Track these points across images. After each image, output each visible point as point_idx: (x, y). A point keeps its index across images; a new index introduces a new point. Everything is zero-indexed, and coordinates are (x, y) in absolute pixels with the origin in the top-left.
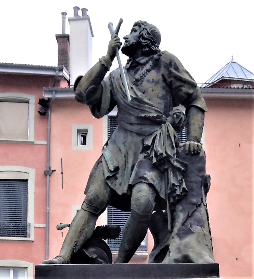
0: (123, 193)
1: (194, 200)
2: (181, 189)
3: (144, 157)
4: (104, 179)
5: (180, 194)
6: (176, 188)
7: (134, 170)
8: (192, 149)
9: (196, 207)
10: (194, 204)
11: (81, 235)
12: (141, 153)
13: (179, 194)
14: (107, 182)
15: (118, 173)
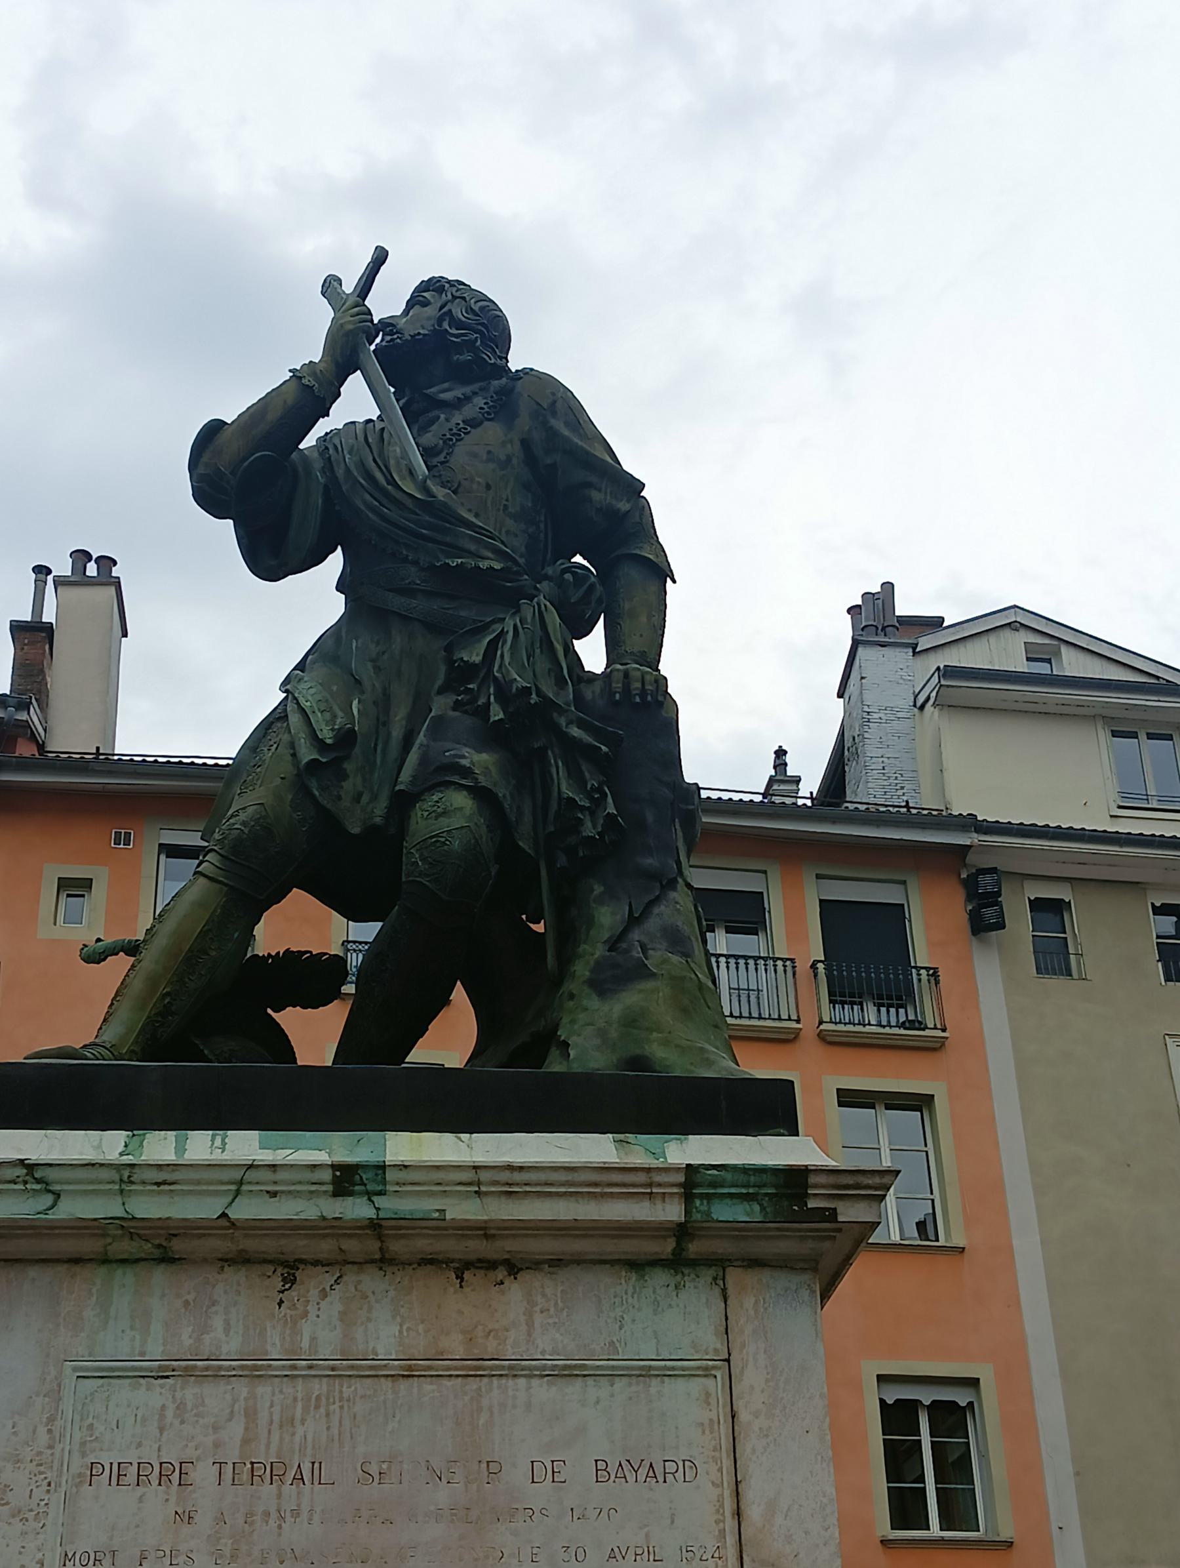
1: (650, 862)
2: (602, 821)
3: (452, 704)
4: (295, 772)
6: (580, 815)
7: (414, 749)
8: (637, 688)
10: (654, 876)
12: (439, 693)
13: (593, 837)
15: (347, 757)
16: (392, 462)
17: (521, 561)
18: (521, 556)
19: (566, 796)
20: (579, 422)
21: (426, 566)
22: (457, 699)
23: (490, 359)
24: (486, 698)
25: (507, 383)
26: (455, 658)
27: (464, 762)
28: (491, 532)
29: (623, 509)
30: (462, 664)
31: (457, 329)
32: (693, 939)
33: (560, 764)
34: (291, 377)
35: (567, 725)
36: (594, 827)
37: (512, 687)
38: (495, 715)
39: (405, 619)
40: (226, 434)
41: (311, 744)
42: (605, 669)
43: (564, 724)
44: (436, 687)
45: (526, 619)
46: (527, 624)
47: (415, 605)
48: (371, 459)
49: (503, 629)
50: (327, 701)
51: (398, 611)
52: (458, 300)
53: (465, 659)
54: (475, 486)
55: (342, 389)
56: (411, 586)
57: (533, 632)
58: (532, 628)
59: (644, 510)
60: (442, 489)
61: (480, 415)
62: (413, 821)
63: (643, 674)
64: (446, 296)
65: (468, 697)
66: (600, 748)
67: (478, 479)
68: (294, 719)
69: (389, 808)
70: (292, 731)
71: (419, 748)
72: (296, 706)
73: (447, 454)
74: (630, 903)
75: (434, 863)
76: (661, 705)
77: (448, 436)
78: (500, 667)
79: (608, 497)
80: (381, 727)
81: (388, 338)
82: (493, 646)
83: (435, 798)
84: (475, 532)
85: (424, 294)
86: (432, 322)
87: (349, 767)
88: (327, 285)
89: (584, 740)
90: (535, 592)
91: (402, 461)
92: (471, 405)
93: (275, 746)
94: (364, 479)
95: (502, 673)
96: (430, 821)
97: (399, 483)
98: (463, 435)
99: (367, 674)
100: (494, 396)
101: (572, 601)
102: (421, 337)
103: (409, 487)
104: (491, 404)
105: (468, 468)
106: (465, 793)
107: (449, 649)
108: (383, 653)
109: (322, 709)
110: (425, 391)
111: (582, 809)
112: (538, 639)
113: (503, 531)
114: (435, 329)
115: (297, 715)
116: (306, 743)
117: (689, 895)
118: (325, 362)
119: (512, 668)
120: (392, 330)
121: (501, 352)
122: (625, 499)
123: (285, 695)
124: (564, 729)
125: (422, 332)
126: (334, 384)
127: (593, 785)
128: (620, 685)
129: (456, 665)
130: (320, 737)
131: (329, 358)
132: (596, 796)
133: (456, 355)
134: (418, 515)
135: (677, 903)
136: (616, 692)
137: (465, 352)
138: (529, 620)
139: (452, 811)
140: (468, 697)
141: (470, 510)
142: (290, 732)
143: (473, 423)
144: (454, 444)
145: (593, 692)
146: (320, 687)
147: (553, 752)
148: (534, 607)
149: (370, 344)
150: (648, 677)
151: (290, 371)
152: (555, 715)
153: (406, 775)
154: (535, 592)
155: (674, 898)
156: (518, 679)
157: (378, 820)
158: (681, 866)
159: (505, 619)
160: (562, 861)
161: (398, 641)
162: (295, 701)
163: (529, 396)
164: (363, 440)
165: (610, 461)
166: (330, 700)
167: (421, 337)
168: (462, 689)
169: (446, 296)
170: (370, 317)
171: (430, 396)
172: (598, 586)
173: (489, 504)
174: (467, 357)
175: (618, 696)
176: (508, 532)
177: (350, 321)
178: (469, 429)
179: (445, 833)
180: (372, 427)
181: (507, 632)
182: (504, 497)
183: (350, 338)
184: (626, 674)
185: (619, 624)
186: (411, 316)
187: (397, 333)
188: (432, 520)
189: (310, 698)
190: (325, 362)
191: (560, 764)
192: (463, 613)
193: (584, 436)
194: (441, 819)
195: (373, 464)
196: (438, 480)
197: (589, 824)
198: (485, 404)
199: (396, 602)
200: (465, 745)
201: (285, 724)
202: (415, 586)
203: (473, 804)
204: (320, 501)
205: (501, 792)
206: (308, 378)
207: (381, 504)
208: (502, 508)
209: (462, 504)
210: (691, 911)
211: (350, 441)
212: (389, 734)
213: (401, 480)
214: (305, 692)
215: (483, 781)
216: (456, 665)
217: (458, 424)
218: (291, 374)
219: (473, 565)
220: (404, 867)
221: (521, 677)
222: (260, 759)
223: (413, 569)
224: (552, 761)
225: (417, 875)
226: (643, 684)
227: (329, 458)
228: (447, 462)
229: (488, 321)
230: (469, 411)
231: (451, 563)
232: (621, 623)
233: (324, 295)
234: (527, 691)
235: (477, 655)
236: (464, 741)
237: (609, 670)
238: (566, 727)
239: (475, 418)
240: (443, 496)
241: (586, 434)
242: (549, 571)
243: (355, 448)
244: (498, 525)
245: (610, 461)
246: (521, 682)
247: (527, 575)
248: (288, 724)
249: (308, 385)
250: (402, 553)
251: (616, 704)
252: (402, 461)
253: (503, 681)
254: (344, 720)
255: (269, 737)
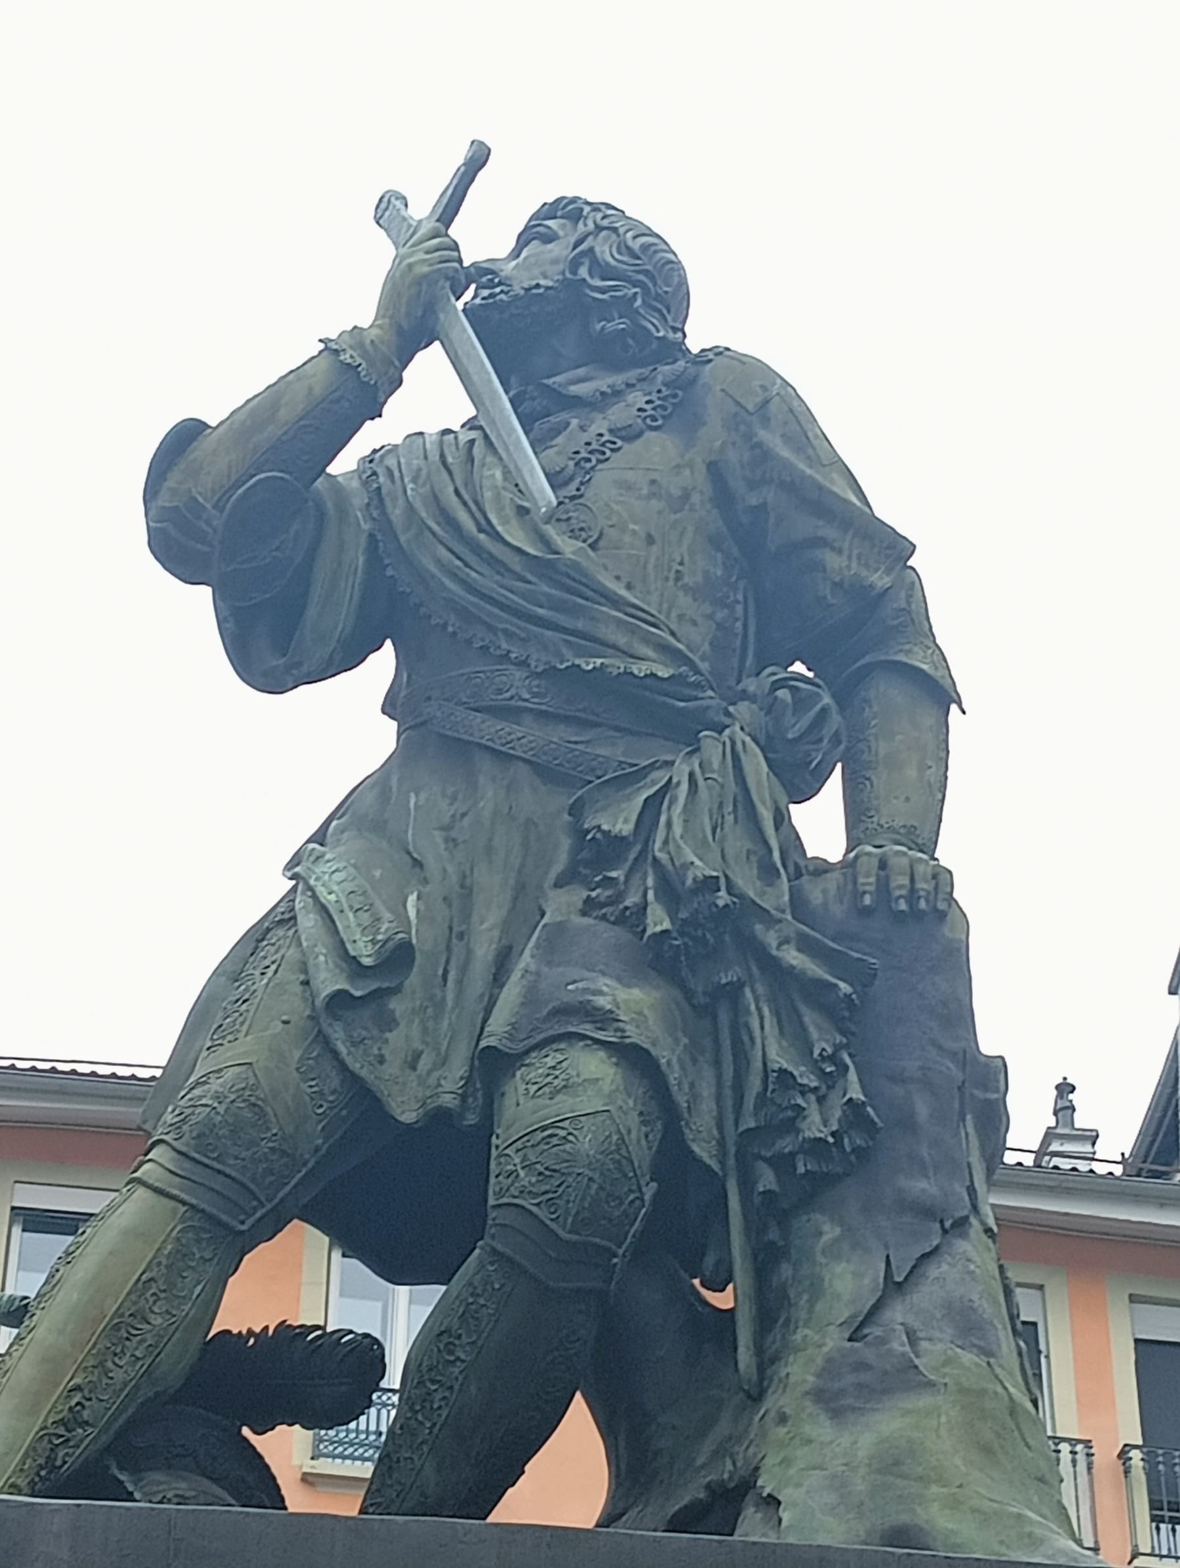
0: (432, 1105)
1: (922, 1187)
2: (838, 1113)
3: (580, 905)
4: (308, 1012)
5: (831, 1140)
6: (800, 1101)
8: (900, 887)
9: (940, 1232)
10: (928, 1212)
11: (115, 1355)
12: (557, 885)
14: (328, 1030)
16: (488, 495)
17: (704, 666)
18: (703, 659)
19: (776, 1067)
20: (808, 438)
21: (539, 670)
22: (589, 896)
23: (658, 331)
24: (640, 894)
25: (686, 368)
26: (586, 826)
27: (601, 1001)
28: (652, 616)
29: (880, 584)
30: (599, 836)
31: (603, 279)
32: (999, 1326)
33: (766, 1012)
34: (320, 352)
35: (780, 945)
36: (825, 1123)
37: (685, 875)
38: (655, 925)
39: (502, 757)
40: (206, 444)
41: (337, 966)
42: (848, 851)
43: (774, 944)
44: (553, 875)
45: (711, 763)
46: (713, 771)
47: (520, 735)
48: (451, 489)
49: (671, 779)
50: (364, 893)
51: (489, 744)
52: (604, 233)
53: (605, 827)
54: (627, 539)
55: (405, 374)
56: (512, 702)
57: (722, 786)
58: (720, 780)
59: (913, 587)
60: (574, 542)
61: (639, 421)
62: (509, 1101)
63: (913, 863)
64: (586, 225)
65: (608, 893)
66: (836, 985)
67: (631, 526)
68: (308, 922)
69: (469, 1080)
70: (305, 944)
71: (523, 976)
72: (310, 900)
73: (582, 483)
74: (888, 1256)
75: (547, 1173)
76: (942, 916)
77: (584, 454)
78: (666, 842)
79: (854, 565)
80: (454, 941)
81: (486, 293)
82: (653, 805)
83: (550, 1061)
84: (626, 614)
85: (549, 223)
86: (561, 267)
87: (396, 1005)
88: (383, 206)
89: (810, 973)
90: (727, 721)
91: (504, 493)
92: (623, 404)
93: (273, 967)
94: (439, 524)
95: (669, 853)
96: (540, 1101)
97: (499, 528)
98: (608, 453)
99: (432, 850)
100: (664, 389)
101: (790, 736)
102: (541, 291)
103: (516, 536)
104: (658, 402)
105: (615, 507)
106: (602, 1054)
107: (576, 810)
108: (464, 815)
109: (357, 906)
110: (545, 381)
111: (804, 1090)
112: (731, 799)
113: (674, 614)
114: (565, 279)
115: (311, 916)
116: (326, 962)
117: (989, 1250)
118: (380, 326)
119: (685, 843)
120: (491, 280)
121: (675, 320)
122: (883, 568)
123: (293, 882)
124: (774, 952)
125: (542, 282)
126: (392, 363)
127: (824, 1049)
128: (872, 880)
129: (589, 837)
130: (352, 953)
131: (387, 320)
132: (828, 1070)
133: (600, 321)
134: (529, 582)
135: (969, 1260)
136: (864, 893)
137: (616, 315)
138: (716, 765)
139: (580, 1084)
140: (608, 893)
141: (618, 578)
142: (300, 945)
143: (629, 434)
144: (592, 468)
145: (825, 891)
146: (352, 870)
147: (753, 991)
148: (724, 744)
149: (458, 299)
150: (920, 869)
151: (320, 341)
152: (758, 928)
153: (498, 1023)
154: (727, 721)
155: (965, 1251)
156: (698, 862)
157: (448, 1101)
158: (976, 1198)
159: (672, 763)
160: (767, 1180)
161: (489, 795)
162: (309, 893)
163: (723, 390)
164: (437, 458)
165: (858, 503)
166: (370, 891)
167: (541, 291)
168: (597, 879)
169: (586, 225)
170: (455, 254)
171: (554, 390)
172: (834, 713)
173: (650, 567)
174: (619, 324)
175: (867, 900)
176: (681, 617)
177: (425, 260)
178: (620, 443)
179: (567, 1122)
180: (453, 441)
181: (678, 783)
182: (679, 560)
183: (424, 287)
184: (883, 864)
185: (868, 779)
186: (526, 258)
187: (500, 284)
188: (554, 592)
189: (335, 888)
190: (380, 326)
191: (766, 1012)
192: (601, 751)
193: (814, 461)
194: (559, 1098)
195: (454, 498)
196: (564, 526)
197: (814, 1113)
198: (647, 402)
199: (488, 729)
200: (603, 973)
201: (291, 933)
202: (521, 703)
203: (615, 1074)
204: (361, 559)
205: (664, 1055)
206: (350, 352)
207: (467, 565)
208: (672, 575)
209: (606, 569)
210: (994, 1278)
211: (415, 462)
212: (469, 952)
213: (503, 524)
214: (326, 877)
215: (635, 1035)
216: (589, 837)
217: (601, 435)
218: (322, 346)
219: (622, 670)
220: (492, 1180)
221: (701, 859)
222: (246, 990)
223: (519, 674)
224: (753, 1007)
225: (517, 1194)
226: (912, 880)
227: (379, 489)
228: (581, 496)
229: (655, 267)
230: (620, 414)
231: (584, 666)
232: (873, 778)
233: (378, 223)
234: (709, 884)
235: (626, 821)
236: (602, 967)
237: (852, 855)
238: (778, 948)
239: (630, 426)
240: (573, 553)
241: (818, 457)
242: (751, 685)
243: (424, 472)
244: (665, 606)
245: (858, 503)
246: (701, 869)
247: (713, 689)
248: (296, 931)
249: (349, 364)
250: (499, 647)
251: (866, 912)
252: (504, 493)
253: (670, 867)
254: (393, 925)
255: (262, 954)
